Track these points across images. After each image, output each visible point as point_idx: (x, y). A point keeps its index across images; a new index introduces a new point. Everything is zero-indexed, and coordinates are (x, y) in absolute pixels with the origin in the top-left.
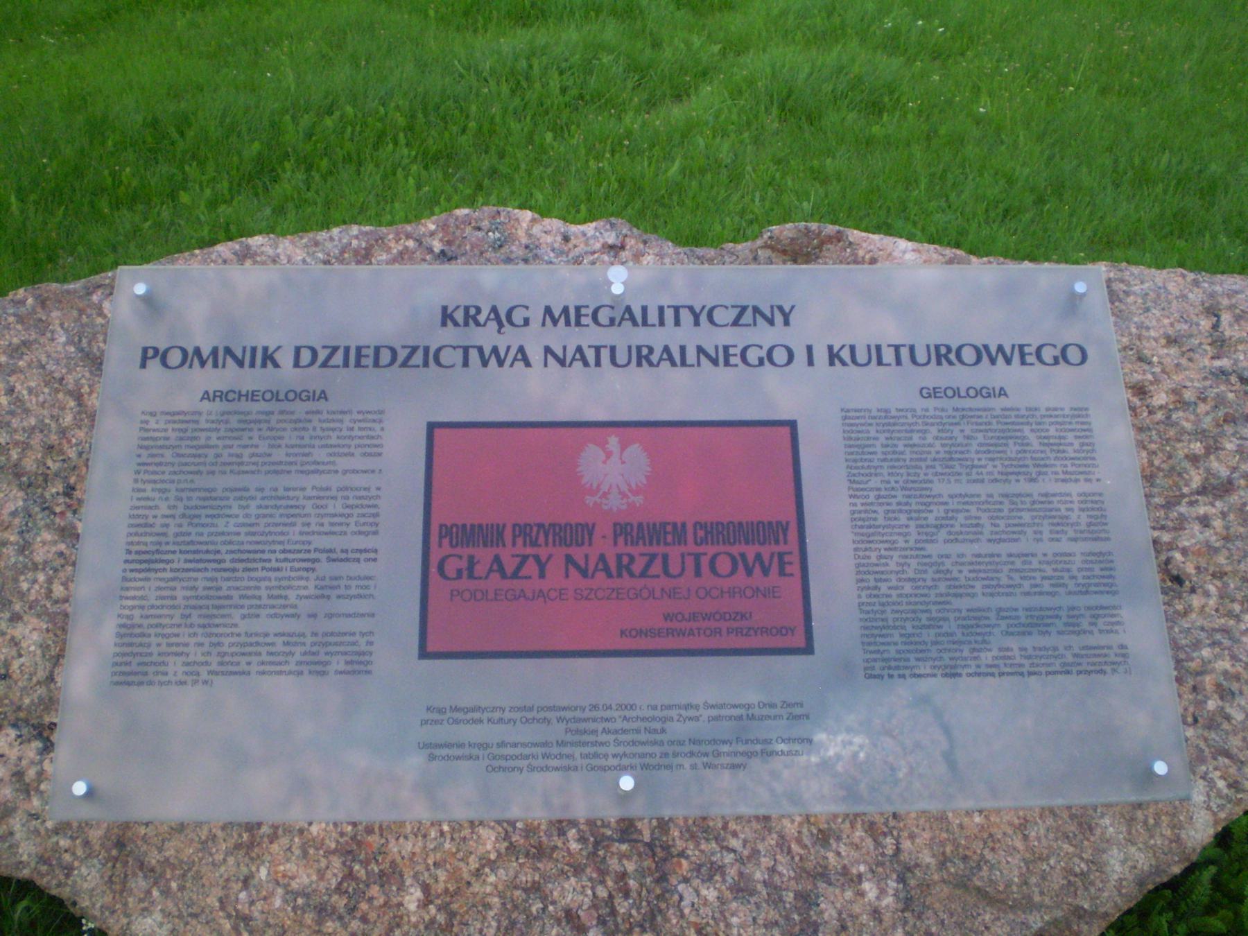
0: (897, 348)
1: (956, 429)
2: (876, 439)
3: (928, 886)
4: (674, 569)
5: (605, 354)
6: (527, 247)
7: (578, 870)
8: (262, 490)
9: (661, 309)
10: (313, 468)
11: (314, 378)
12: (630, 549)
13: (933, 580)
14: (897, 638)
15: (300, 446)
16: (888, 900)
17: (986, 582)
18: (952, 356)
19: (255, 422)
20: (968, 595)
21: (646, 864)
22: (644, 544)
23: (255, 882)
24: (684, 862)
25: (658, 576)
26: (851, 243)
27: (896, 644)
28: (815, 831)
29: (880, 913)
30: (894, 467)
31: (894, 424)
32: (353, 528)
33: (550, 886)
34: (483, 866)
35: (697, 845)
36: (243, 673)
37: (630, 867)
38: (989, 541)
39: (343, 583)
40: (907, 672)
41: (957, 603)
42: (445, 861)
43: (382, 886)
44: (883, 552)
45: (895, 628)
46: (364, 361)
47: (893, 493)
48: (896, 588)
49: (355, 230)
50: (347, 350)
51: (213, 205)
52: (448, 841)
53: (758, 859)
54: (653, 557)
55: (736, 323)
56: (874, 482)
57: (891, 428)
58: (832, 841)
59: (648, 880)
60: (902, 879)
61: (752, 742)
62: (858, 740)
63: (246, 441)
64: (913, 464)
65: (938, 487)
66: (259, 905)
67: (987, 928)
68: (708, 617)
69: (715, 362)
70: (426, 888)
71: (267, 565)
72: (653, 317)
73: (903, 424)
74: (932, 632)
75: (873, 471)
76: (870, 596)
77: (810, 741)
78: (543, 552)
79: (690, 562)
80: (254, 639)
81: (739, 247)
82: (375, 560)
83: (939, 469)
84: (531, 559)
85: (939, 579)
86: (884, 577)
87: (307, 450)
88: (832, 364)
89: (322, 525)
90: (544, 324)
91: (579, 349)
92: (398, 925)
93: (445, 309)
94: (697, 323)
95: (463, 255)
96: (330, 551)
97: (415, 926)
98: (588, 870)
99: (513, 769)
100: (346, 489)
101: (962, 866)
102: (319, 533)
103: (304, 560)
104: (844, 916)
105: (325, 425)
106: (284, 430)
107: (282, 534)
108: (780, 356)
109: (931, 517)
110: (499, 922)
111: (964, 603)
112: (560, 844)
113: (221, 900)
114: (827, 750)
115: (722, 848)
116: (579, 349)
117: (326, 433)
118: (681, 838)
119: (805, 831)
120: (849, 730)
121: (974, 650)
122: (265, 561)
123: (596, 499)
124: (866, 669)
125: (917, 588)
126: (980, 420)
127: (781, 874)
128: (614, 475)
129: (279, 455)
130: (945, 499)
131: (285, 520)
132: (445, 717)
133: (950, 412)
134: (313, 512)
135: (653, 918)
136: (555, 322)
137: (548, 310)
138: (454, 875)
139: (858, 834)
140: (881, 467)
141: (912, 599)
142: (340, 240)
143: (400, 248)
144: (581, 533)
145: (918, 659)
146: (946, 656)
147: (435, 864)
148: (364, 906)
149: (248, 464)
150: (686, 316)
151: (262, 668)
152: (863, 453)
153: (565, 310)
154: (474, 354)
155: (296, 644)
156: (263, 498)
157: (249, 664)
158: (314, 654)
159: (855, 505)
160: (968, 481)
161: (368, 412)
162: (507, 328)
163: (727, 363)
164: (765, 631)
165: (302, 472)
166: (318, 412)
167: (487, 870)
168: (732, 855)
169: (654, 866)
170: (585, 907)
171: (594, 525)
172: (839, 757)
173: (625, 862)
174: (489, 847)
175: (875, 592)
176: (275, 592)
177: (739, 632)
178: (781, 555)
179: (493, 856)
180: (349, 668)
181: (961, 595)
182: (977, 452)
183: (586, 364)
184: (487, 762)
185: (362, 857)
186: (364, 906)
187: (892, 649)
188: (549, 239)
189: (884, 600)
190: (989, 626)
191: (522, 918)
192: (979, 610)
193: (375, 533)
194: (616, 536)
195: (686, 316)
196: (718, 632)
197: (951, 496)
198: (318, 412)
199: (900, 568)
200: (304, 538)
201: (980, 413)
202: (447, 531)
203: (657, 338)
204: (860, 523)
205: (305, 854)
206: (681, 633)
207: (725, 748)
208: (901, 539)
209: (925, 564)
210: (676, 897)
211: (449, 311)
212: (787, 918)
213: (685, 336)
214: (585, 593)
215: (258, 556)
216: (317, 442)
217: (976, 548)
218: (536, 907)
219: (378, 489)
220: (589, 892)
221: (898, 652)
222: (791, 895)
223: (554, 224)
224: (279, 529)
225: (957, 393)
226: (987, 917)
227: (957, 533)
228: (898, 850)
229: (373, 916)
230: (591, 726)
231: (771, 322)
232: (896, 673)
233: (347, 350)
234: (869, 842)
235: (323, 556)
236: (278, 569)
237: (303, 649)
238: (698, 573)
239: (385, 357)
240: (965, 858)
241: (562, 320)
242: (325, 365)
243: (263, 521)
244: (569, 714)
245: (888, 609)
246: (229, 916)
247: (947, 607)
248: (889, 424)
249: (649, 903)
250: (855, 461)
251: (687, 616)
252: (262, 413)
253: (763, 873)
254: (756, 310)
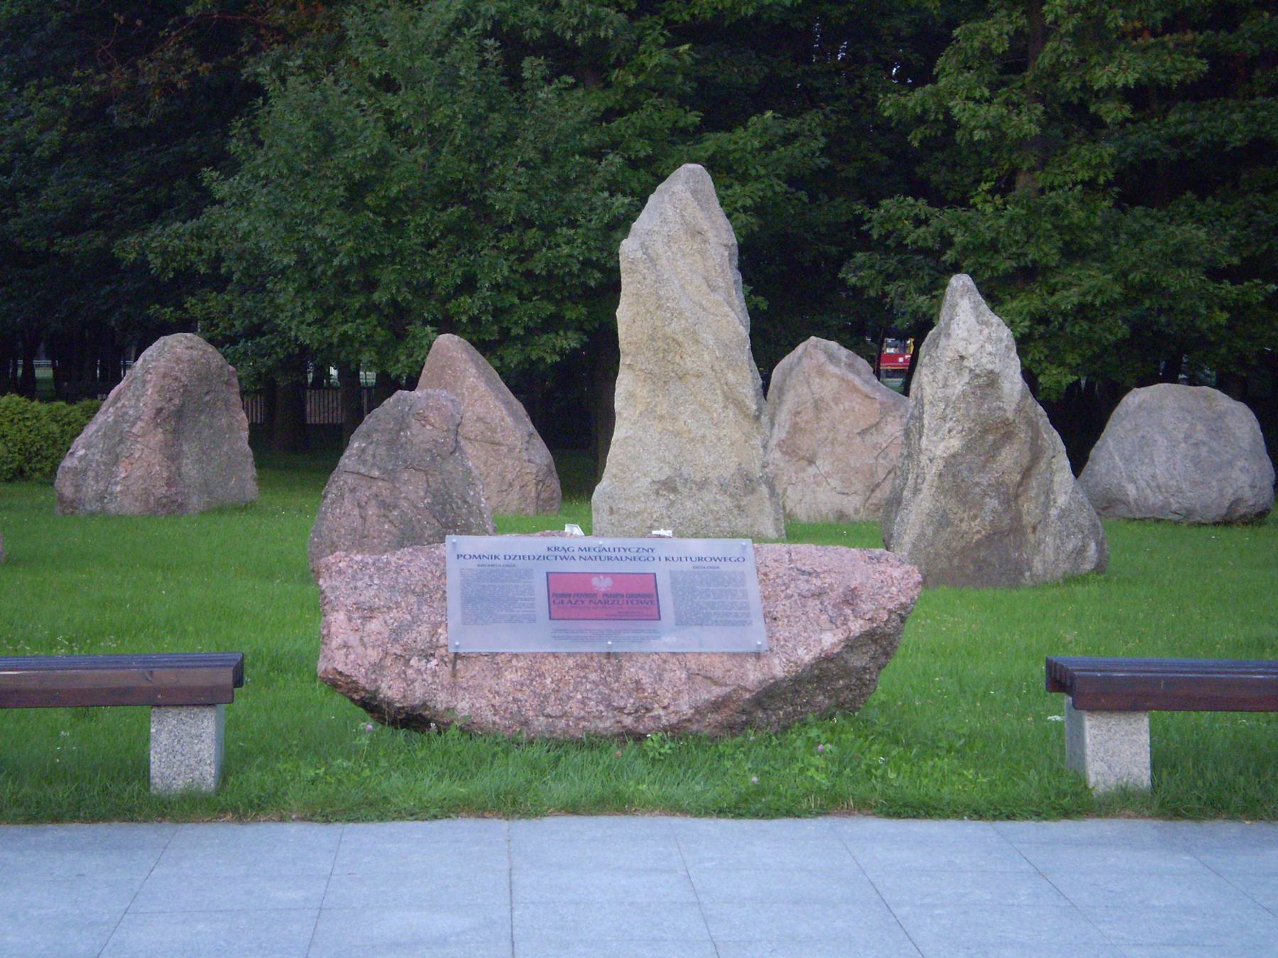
11: (511, 562)
128: (602, 585)
144: (595, 595)
203: (613, 555)
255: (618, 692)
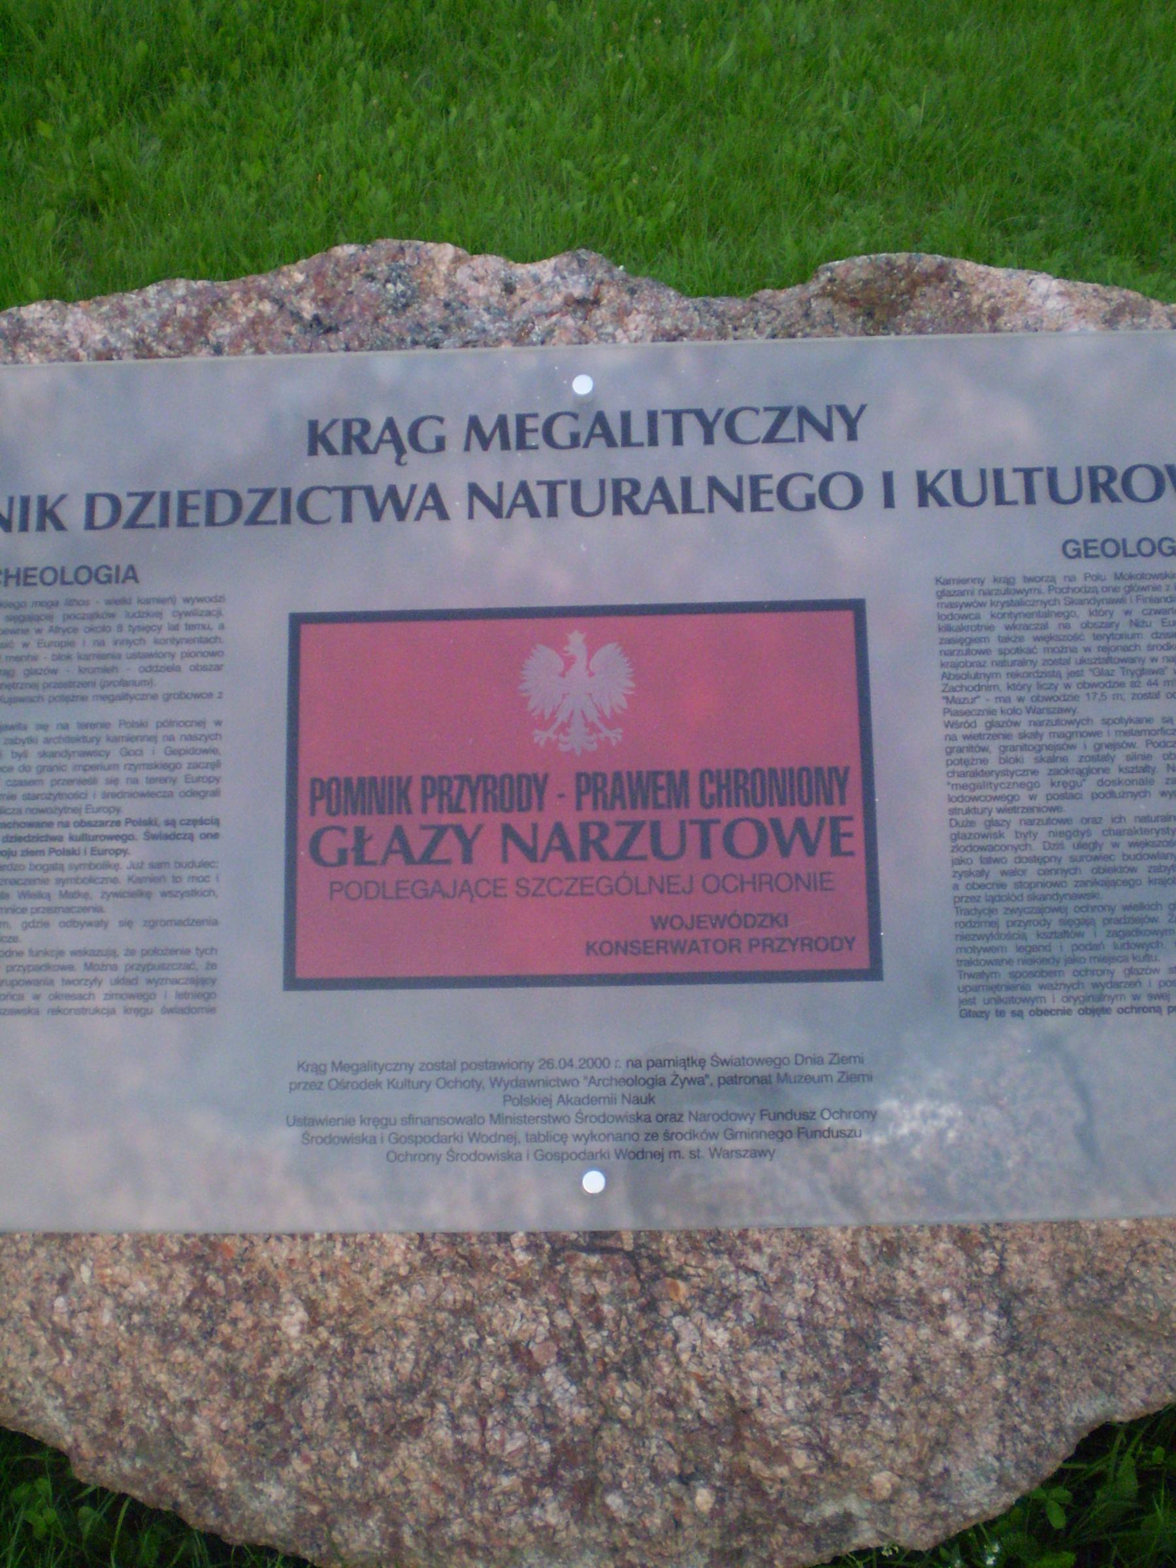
0: (1028, 474)
1: (1118, 609)
2: (990, 628)
3: (1044, 1317)
4: (669, 845)
5: (564, 495)
6: (447, 305)
7: (528, 1289)
8: (44, 727)
9: (652, 417)
10: (119, 691)
12: (604, 816)
13: (1073, 859)
14: (1011, 953)
15: (100, 657)
16: (984, 1341)
17: (1155, 863)
18: (1116, 486)
19: (31, 618)
20: (1125, 883)
21: (626, 1284)
22: (624, 807)
23: (75, 1284)
24: (682, 1285)
25: (643, 858)
26: (960, 284)
27: (1009, 962)
28: (878, 1241)
29: (971, 1358)
30: (1017, 675)
31: (1020, 603)
32: (182, 786)
33: (488, 1309)
34: (391, 1283)
35: (703, 1259)
36: (29, 1011)
37: (603, 1288)
38: (1163, 794)
39: (167, 872)
40: (1026, 1008)
41: (1109, 896)
42: (336, 1272)
43: (249, 1302)
44: (996, 816)
45: (1009, 937)
46: (192, 516)
47: (1014, 718)
48: (1014, 873)
49: (181, 287)
50: (165, 497)
51: (83, 138)
52: (339, 1245)
53: (791, 1286)
54: (636, 827)
55: (770, 438)
56: (986, 700)
57: (1015, 610)
58: (903, 1255)
59: (630, 1306)
60: (1005, 1311)
61: (784, 1116)
62: (947, 1110)
63: (19, 651)
64: (1049, 668)
65: (1086, 708)
66: (82, 1318)
67: (1130, 1368)
68: (721, 921)
69: (737, 505)
70: (311, 1306)
71: (57, 845)
72: (639, 431)
73: (1034, 603)
74: (1067, 943)
75: (983, 682)
76: (972, 886)
77: (873, 1115)
78: (469, 822)
79: (693, 832)
80: (42, 960)
81: (782, 295)
82: (216, 836)
83: (1089, 678)
84: (450, 833)
85: (1082, 859)
86: (994, 855)
87: (109, 663)
88: (923, 503)
89: (136, 781)
90: (467, 448)
91: (523, 488)
92: (276, 1353)
93: (313, 425)
94: (709, 439)
95: (347, 323)
96: (150, 822)
97: (300, 1354)
98: (543, 1290)
99: (426, 1157)
100: (171, 723)
101: (1097, 1286)
102: (132, 795)
103: (111, 838)
104: (918, 1362)
105: (135, 622)
106: (75, 630)
107: (77, 796)
108: (841, 492)
109: (1073, 756)
110: (417, 1353)
111: (1115, 897)
112: (500, 1255)
113: (32, 1305)
114: (898, 1125)
115: (739, 1267)
116: (523, 488)
117: (138, 635)
118: (678, 1249)
119: (863, 1241)
120: (933, 1095)
121: (1131, 971)
122: (53, 839)
123: (550, 734)
124: (961, 1002)
125: (1047, 872)
126: (1156, 594)
127: (824, 1309)
128: (580, 694)
129: (68, 671)
130: (1097, 726)
131: (80, 774)
132: (325, 1078)
133: (1112, 583)
134: (123, 761)
135: (637, 1360)
136: (485, 443)
137: (474, 424)
138: (350, 1290)
139: (942, 1246)
140: (997, 675)
141: (1039, 891)
142: (159, 304)
143: (251, 315)
144: (525, 790)
145: (1042, 987)
146: (1088, 980)
147: (323, 1274)
148: (225, 1329)
149: (23, 686)
150: (691, 425)
151: (56, 1004)
152: (968, 652)
153: (502, 422)
154: (359, 499)
155: (103, 967)
156: (47, 741)
157: (37, 997)
158: (130, 982)
159: (953, 738)
160: (1135, 697)
161: (200, 600)
162: (411, 455)
163: (756, 507)
164: (808, 943)
165: (104, 698)
166: (124, 601)
167: (396, 1287)
168: (752, 1279)
169: (638, 1287)
170: (539, 1339)
171: (546, 776)
172: (916, 1136)
173: (596, 1281)
174: (397, 1258)
175: (980, 880)
176: (71, 888)
177: (766, 944)
178: (835, 821)
179: (403, 1271)
180: (183, 1003)
181: (1114, 884)
182: (1151, 648)
183: (534, 513)
184: (388, 1146)
185: (218, 1263)
186: (225, 1329)
187: (1004, 970)
188: (482, 290)
189: (992, 893)
190: (1155, 932)
191: (449, 1350)
192: (1142, 907)
193: (216, 793)
194: (580, 793)
195: (691, 425)
196: (732, 945)
197: (1106, 722)
198: (124, 601)
199: (1020, 842)
200: (111, 802)
201: (1158, 582)
202: (322, 789)
203: (641, 465)
204: (960, 768)
205: (139, 1256)
206: (679, 947)
207: (743, 1125)
208: (1023, 793)
209: (1061, 834)
210: (669, 1336)
211: (321, 428)
212: (833, 1368)
213: (695, 459)
214: (533, 886)
215: (43, 831)
216: (124, 650)
217: (1141, 807)
218: (469, 1338)
219: (218, 723)
220: (545, 1319)
221: (1013, 975)
222: (840, 1336)
223: (492, 264)
224: (73, 789)
225: (1121, 548)
226: (1131, 1352)
227: (1113, 783)
228: (1001, 1269)
229: (238, 1342)
230: (540, 1092)
231: (827, 435)
232: (1009, 1008)
233: (165, 497)
234: (960, 1259)
235: (140, 831)
236: (73, 852)
237: (114, 975)
238: (706, 853)
239: (224, 508)
240: (1101, 1275)
241: (497, 440)
242: (132, 524)
243: (47, 777)
244: (507, 1075)
245: (999, 905)
246: (44, 1328)
247: (1093, 902)
248: (1010, 604)
249: (630, 1339)
250: (956, 665)
251: (688, 922)
252: (41, 604)
253: (798, 1305)
254: (804, 415)
255: (638, 1434)
